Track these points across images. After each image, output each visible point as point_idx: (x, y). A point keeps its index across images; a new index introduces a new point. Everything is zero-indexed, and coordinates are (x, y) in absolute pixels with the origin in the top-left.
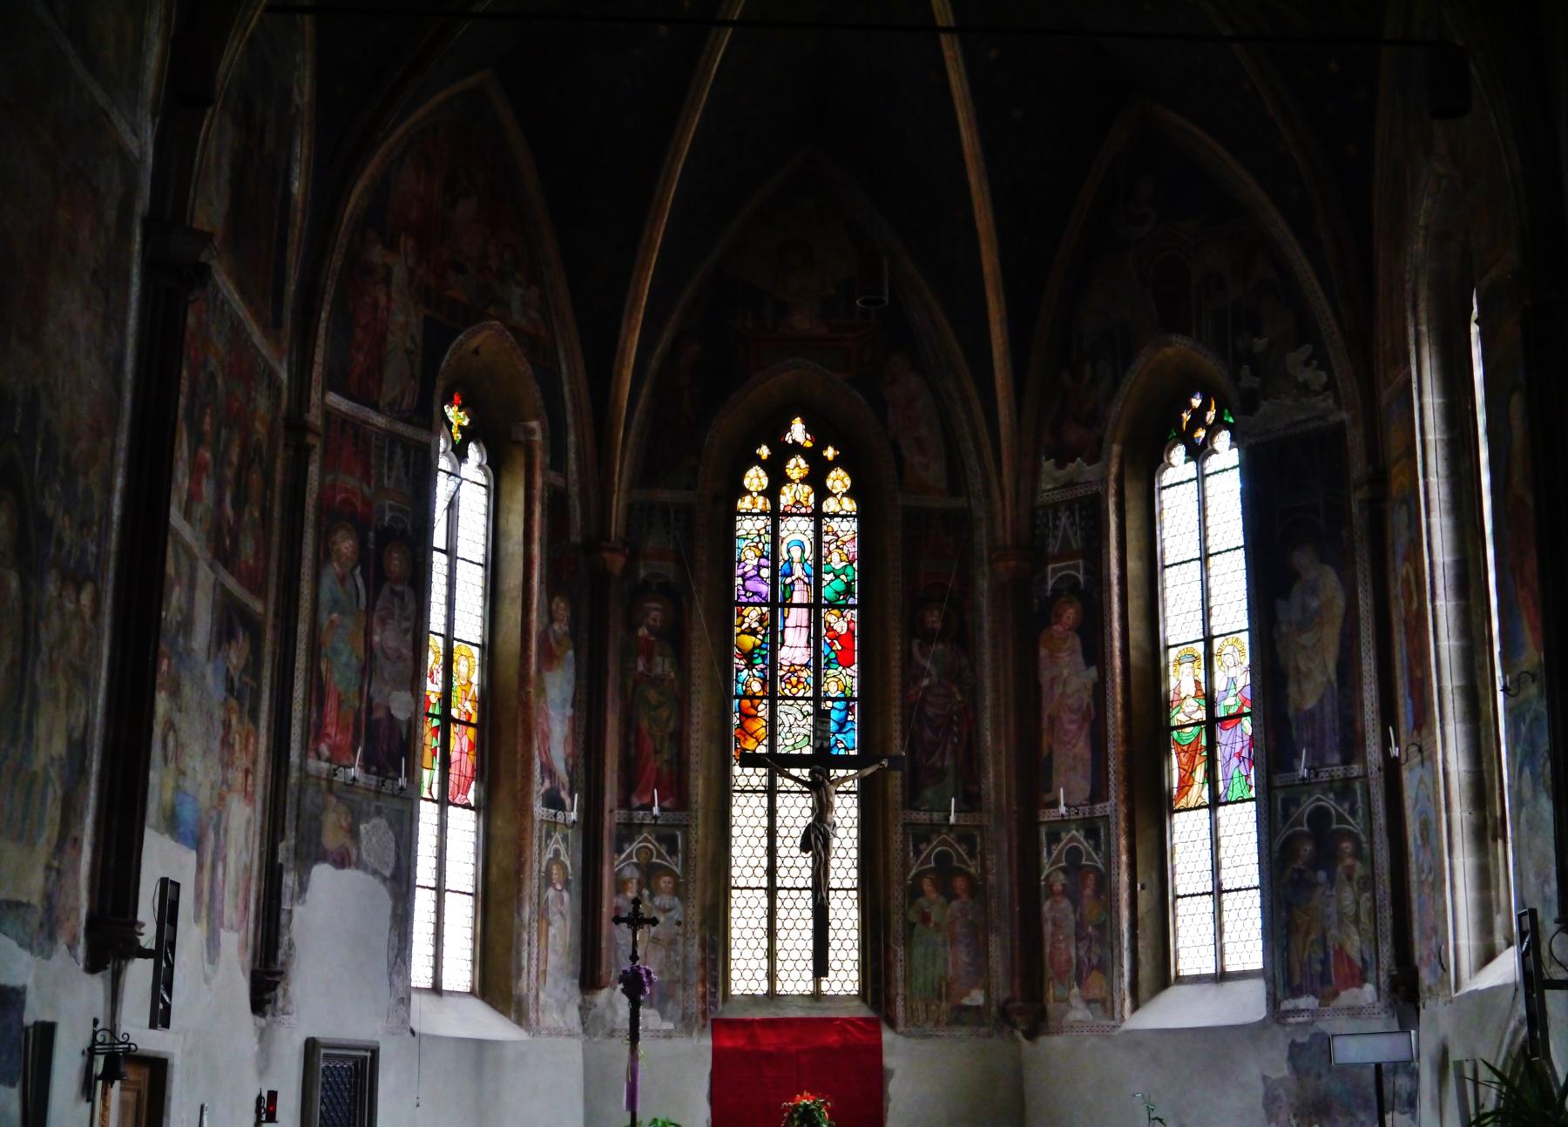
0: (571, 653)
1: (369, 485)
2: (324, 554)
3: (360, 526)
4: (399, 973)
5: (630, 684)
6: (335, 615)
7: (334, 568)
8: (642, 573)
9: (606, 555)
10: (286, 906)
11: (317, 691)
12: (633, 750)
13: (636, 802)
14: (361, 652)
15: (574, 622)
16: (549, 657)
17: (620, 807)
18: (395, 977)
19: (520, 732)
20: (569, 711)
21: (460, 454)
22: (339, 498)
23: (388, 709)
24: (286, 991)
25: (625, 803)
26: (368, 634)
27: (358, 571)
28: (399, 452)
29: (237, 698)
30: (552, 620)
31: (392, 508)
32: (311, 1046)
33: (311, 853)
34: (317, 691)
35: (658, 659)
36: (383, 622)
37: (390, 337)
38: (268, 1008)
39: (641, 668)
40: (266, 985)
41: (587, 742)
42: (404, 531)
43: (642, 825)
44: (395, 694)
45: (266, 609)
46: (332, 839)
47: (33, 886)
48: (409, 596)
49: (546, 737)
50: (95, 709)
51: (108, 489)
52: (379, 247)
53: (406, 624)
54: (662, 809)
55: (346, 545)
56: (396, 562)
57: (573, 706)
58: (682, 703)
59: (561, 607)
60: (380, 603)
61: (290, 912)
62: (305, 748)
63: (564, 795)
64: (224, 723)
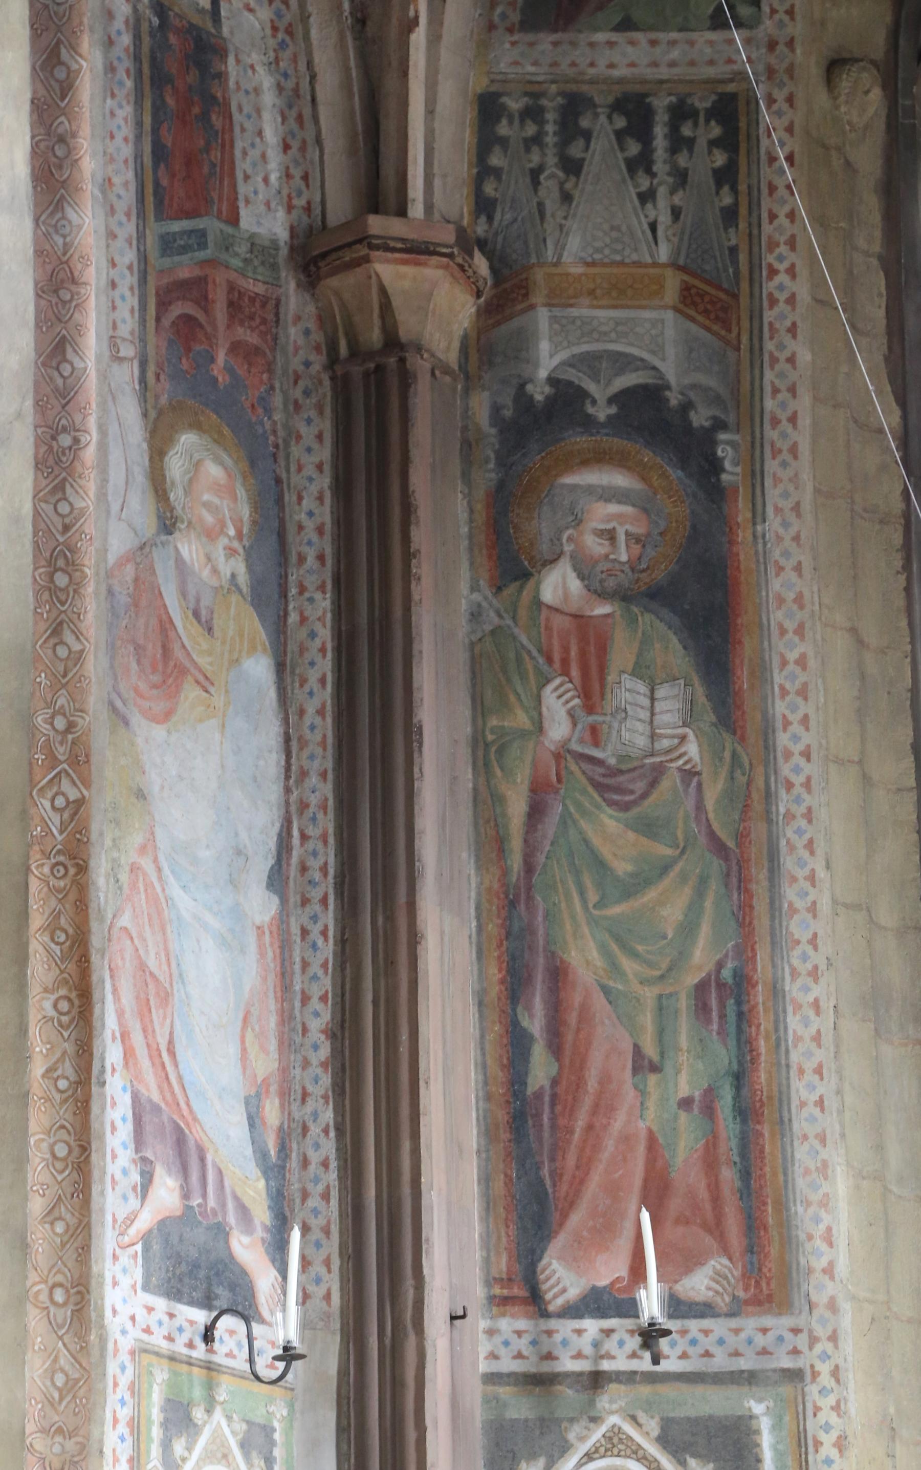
0: (259, 669)
5: (517, 807)
8: (547, 358)
9: (389, 271)
12: (541, 1070)
13: (563, 1279)
15: (271, 536)
16: (168, 668)
17: (500, 1303)
19: (41, 968)
20: (261, 906)
25: (522, 1291)
30: (168, 523)
35: (628, 691)
39: (558, 728)
41: (345, 1029)
43: (596, 1380)
49: (156, 993)
54: (677, 1306)
57: (277, 879)
58: (739, 863)
59: (207, 473)
63: (248, 1250)
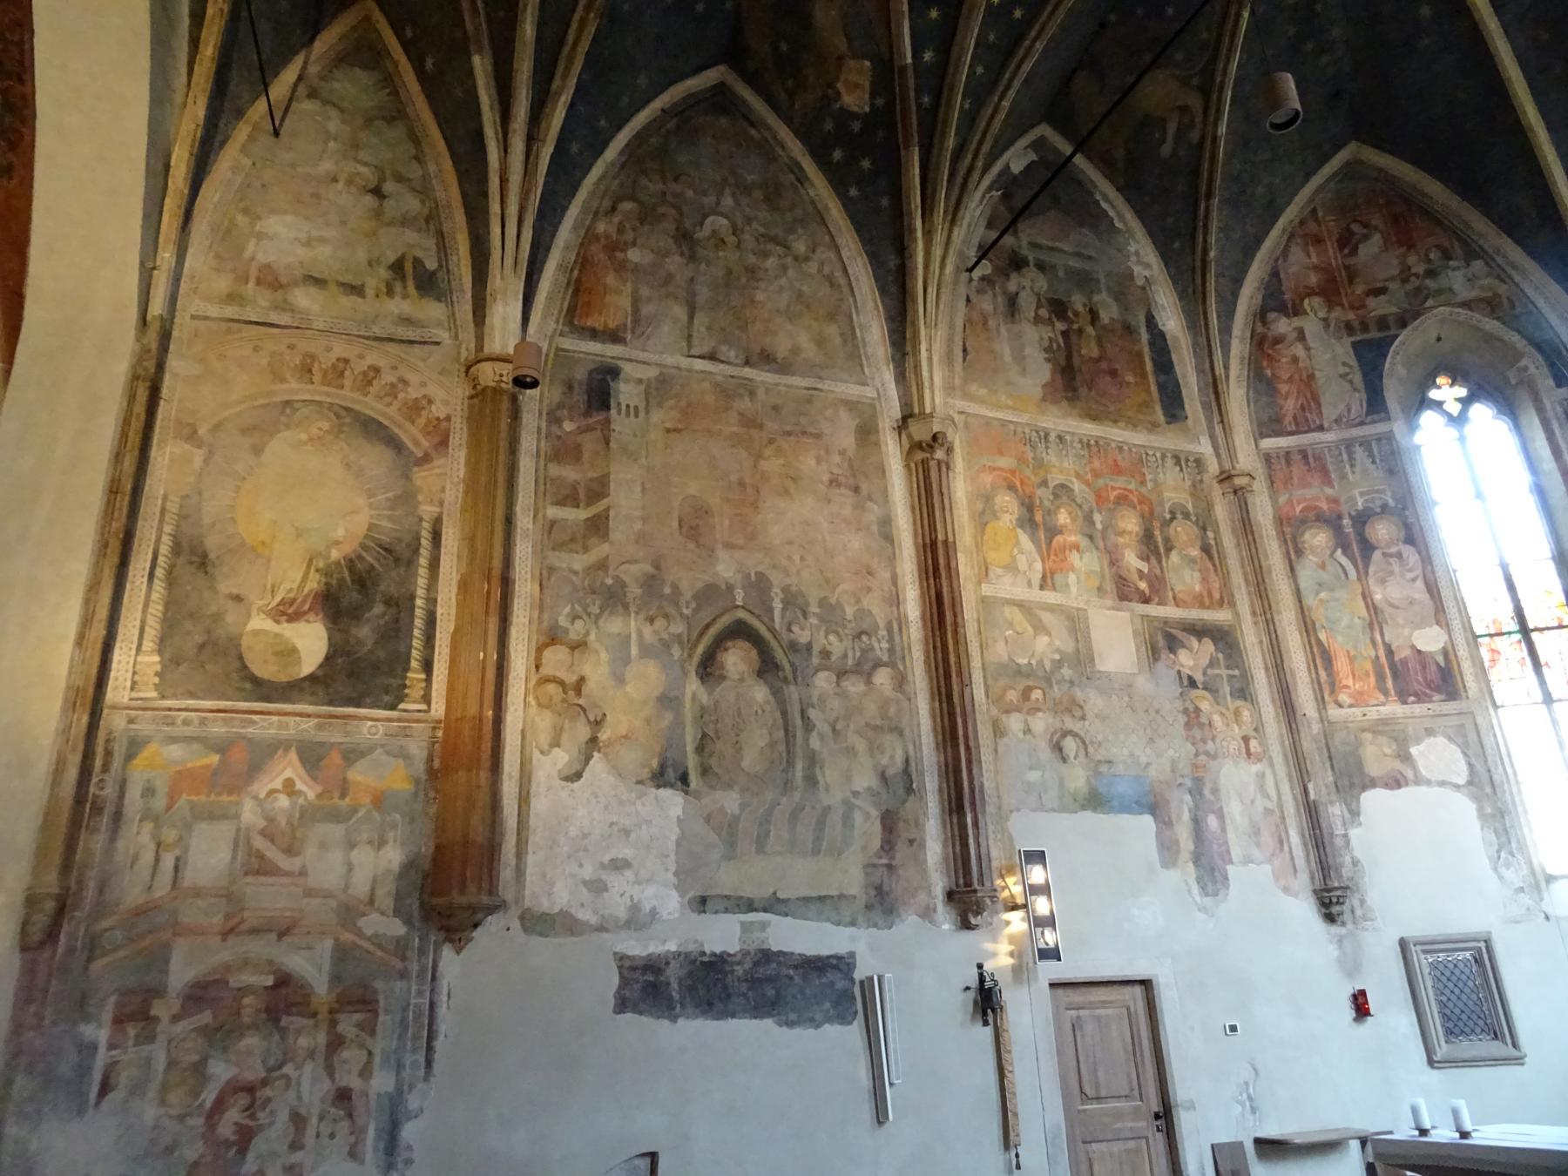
1: (1332, 487)
2: (1294, 552)
3: (1332, 522)
4: (1508, 866)
6: (1323, 595)
7: (1311, 560)
10: (1339, 831)
11: (1322, 657)
14: (1364, 613)
18: (1503, 870)
21: (1458, 421)
22: (1298, 509)
23: (1413, 647)
24: (1362, 902)
26: (1366, 596)
27: (1339, 551)
28: (1359, 453)
29: (1205, 688)
31: (1362, 494)
32: (1403, 944)
33: (1353, 780)
34: (1322, 657)
36: (1383, 581)
37: (1318, 374)
38: (1347, 916)
40: (1331, 901)
42: (1384, 507)
44: (1416, 633)
45: (1237, 615)
46: (1374, 768)
47: (850, 877)
48: (1410, 553)
50: (918, 746)
51: (896, 600)
52: (1284, 320)
53: (1410, 575)
55: (1318, 539)
56: (1382, 531)
60: (1371, 570)
61: (1346, 836)
62: (1321, 703)
64: (1186, 711)
